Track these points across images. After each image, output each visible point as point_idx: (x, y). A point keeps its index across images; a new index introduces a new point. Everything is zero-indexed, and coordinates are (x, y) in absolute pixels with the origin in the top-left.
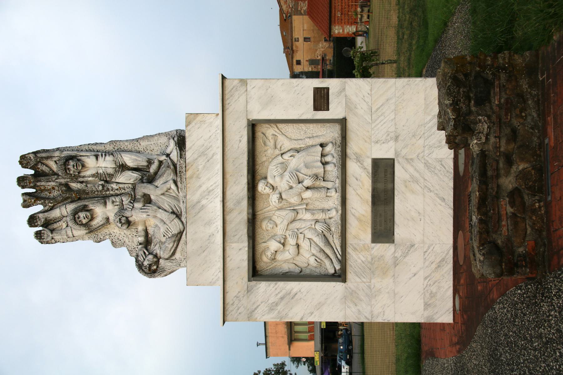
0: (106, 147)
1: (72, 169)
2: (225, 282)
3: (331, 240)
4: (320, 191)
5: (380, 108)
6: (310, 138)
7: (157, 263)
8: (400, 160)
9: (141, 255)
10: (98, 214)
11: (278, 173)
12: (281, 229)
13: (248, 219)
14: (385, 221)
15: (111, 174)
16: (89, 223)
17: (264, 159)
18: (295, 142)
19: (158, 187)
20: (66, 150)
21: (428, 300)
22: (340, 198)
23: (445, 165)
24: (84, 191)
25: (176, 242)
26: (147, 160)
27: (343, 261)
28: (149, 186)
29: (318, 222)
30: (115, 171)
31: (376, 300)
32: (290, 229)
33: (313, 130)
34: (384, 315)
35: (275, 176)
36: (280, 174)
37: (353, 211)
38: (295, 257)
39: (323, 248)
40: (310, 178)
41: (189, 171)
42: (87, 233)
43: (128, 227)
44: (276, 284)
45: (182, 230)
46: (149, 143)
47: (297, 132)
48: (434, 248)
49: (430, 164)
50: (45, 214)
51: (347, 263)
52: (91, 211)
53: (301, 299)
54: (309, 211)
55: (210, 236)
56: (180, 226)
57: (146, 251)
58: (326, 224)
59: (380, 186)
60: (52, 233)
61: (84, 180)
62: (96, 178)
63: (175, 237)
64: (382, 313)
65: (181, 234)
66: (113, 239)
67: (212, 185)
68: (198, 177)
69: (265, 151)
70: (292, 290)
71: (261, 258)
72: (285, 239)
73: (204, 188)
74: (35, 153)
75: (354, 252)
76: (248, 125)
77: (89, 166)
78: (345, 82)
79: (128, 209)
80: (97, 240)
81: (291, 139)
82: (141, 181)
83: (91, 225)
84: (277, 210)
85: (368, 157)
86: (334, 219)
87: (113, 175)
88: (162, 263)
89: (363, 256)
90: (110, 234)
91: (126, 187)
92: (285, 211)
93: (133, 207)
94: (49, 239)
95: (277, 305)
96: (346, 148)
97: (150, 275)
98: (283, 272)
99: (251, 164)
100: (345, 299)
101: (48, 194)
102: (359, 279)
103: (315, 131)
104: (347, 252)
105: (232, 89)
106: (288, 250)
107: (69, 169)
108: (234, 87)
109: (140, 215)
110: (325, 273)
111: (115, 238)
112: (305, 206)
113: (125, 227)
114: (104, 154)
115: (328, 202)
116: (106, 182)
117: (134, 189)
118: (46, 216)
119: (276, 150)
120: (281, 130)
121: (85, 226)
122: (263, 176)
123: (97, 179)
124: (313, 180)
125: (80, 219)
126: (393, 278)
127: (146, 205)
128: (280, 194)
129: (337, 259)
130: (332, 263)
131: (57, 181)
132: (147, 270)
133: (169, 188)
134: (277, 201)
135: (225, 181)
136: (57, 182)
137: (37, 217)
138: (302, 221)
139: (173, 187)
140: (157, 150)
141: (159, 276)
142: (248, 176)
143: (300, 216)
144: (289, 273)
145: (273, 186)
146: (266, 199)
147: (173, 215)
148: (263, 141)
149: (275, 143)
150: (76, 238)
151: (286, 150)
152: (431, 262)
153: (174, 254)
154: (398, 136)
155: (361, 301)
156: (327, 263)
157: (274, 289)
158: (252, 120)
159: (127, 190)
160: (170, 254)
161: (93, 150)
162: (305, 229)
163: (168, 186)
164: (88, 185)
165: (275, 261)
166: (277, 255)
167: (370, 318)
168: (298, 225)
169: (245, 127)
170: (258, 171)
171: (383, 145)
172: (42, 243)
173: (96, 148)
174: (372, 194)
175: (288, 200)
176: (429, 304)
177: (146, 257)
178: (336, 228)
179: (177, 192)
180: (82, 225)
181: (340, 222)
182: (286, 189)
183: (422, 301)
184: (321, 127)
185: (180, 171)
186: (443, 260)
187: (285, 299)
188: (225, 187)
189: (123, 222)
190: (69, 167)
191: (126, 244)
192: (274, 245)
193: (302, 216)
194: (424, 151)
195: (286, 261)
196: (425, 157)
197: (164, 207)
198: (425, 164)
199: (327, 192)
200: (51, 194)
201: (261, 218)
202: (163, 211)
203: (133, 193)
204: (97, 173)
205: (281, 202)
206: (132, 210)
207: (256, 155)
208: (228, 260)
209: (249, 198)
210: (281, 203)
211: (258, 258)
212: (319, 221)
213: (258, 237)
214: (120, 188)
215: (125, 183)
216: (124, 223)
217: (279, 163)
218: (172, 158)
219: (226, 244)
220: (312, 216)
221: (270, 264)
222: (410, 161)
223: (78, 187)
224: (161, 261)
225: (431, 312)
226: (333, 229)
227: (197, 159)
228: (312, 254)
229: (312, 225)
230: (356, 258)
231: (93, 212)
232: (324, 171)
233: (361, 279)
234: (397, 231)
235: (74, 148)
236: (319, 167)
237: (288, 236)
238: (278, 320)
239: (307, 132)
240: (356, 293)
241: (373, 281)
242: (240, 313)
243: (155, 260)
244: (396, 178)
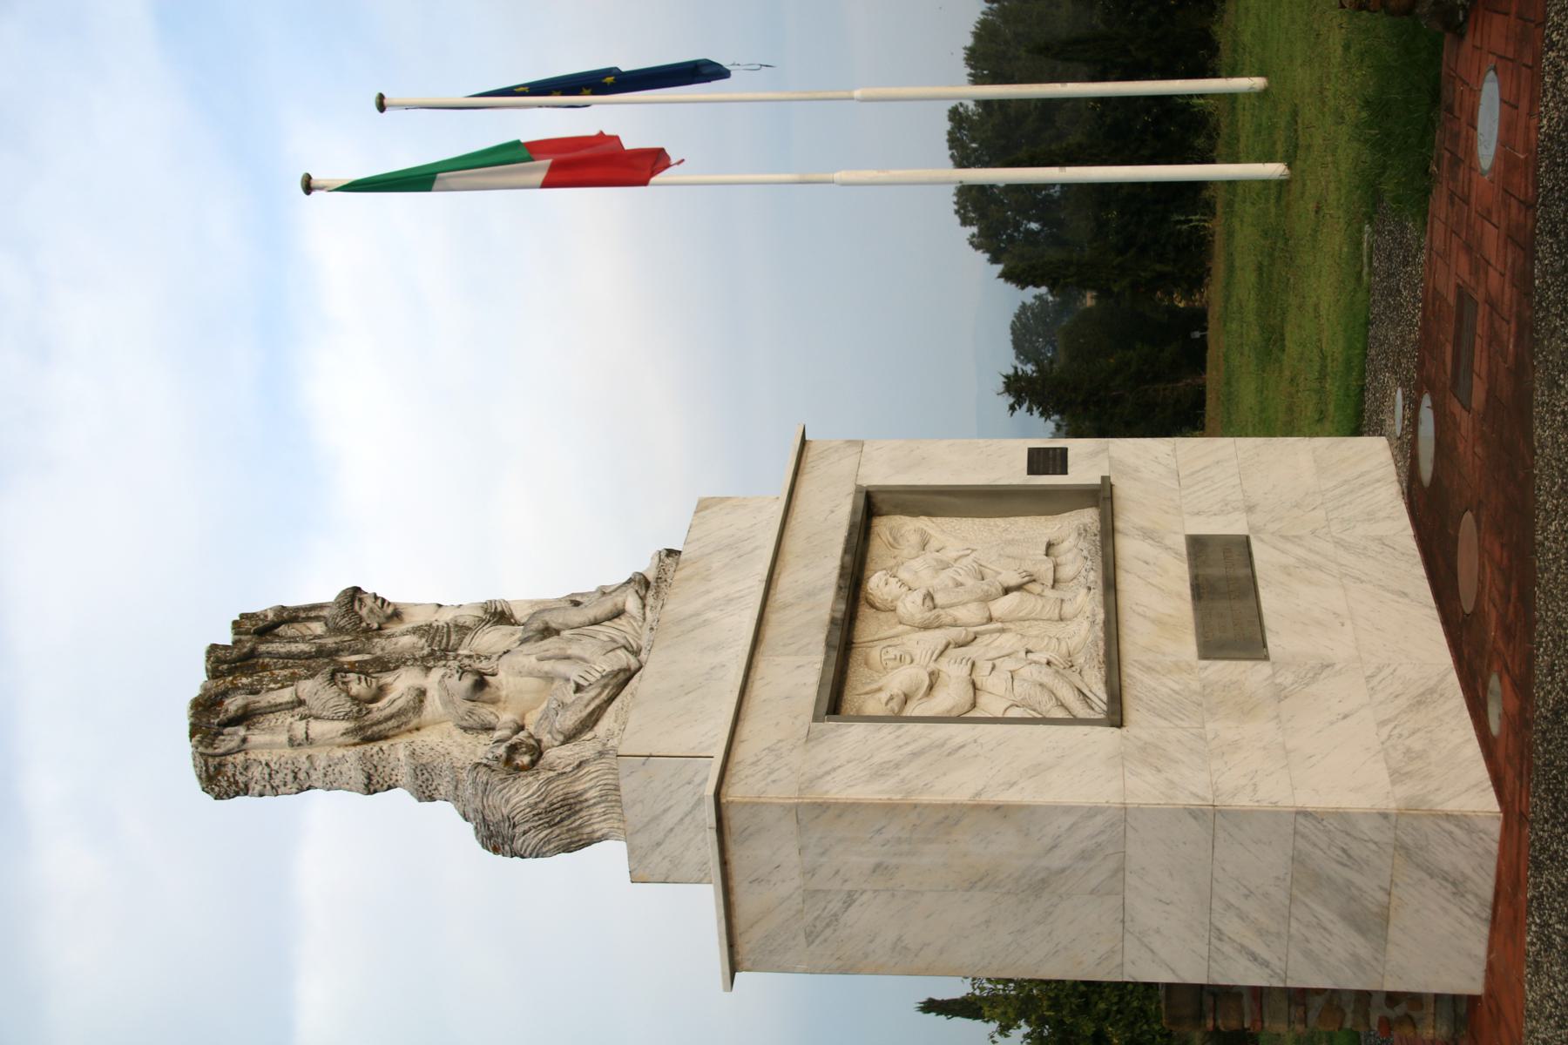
2: (740, 723)
5: (1199, 471)
13: (833, 621)
21: (1403, 764)
25: (610, 687)
31: (1226, 763)
34: (1255, 790)
44: (900, 728)
48: (1395, 670)
55: (712, 669)
59: (1215, 571)
65: (628, 674)
67: (740, 591)
75: (1146, 676)
87: (469, 629)
95: (897, 766)
100: (1123, 758)
107: (361, 600)
135: (779, 563)
142: (843, 558)
153: (590, 721)
155: (1177, 762)
157: (893, 736)
167: (1210, 797)
174: (1192, 585)
176: (1407, 773)
181: (1101, 635)
186: (1432, 691)
209: (840, 588)
233: (1170, 722)
238: (897, 797)
241: (1210, 726)
242: (774, 781)
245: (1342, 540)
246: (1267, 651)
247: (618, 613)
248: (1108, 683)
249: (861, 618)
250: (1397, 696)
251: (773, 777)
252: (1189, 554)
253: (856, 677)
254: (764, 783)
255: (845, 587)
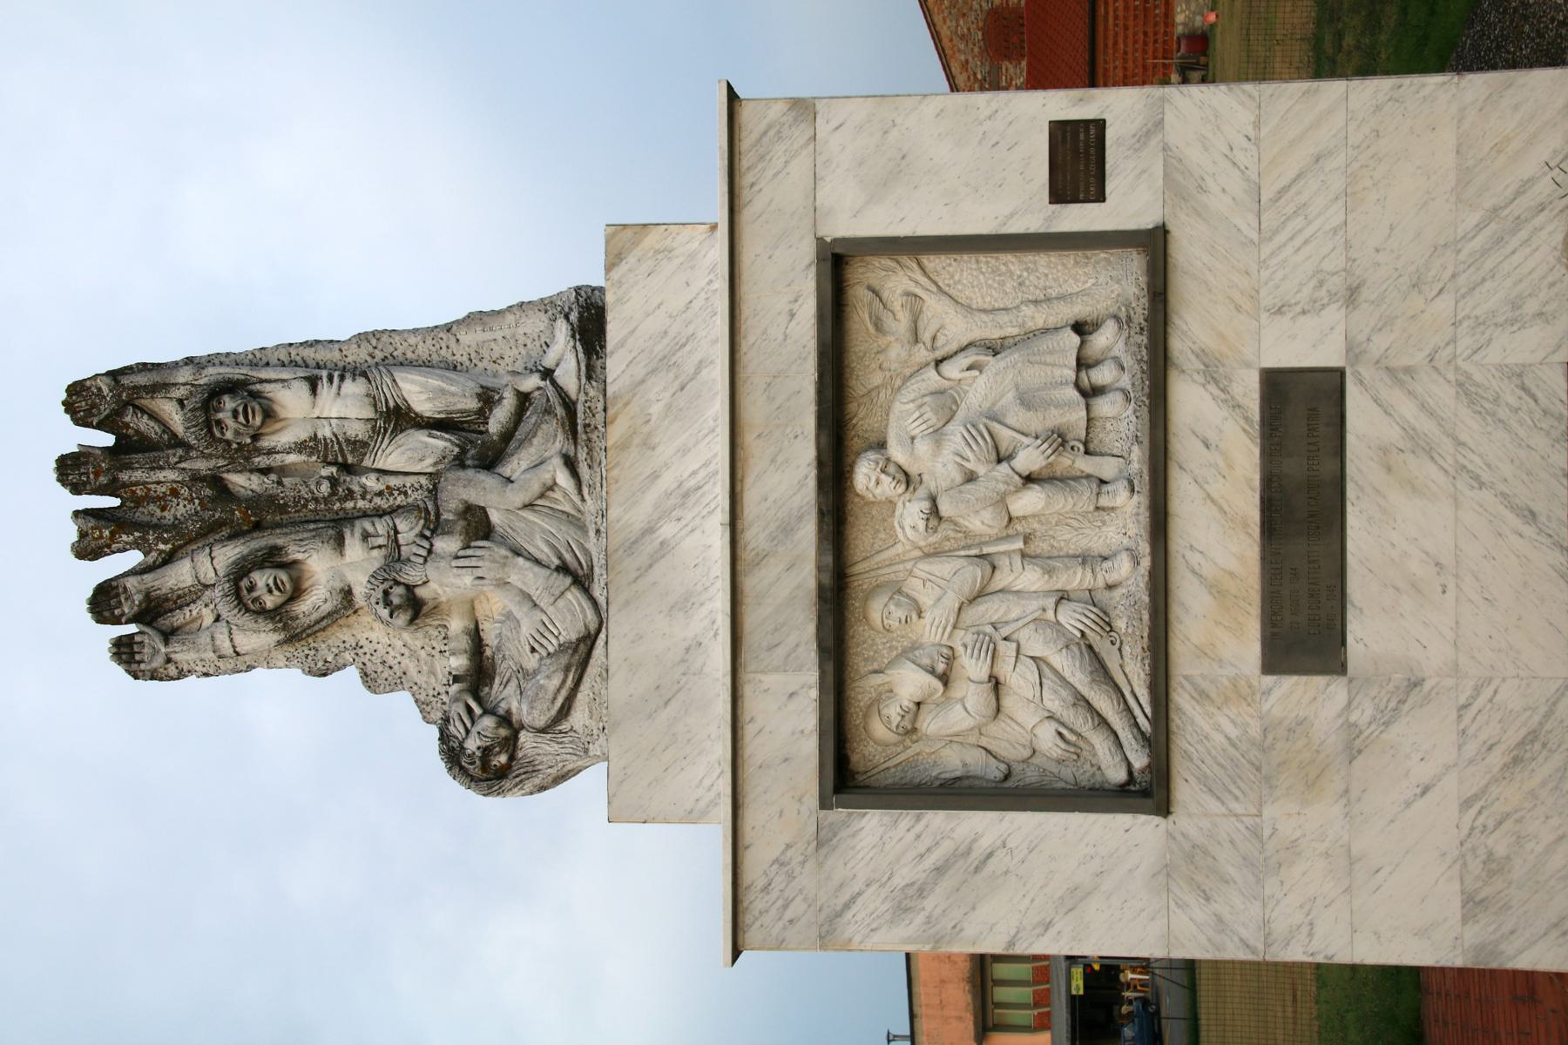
0: (344, 353)
1: (230, 422)
2: (740, 812)
3: (1113, 664)
4: (1073, 490)
6: (1036, 302)
7: (511, 743)
8: (1366, 372)
9: (456, 718)
10: (316, 576)
11: (924, 426)
12: (936, 623)
13: (821, 588)
14: (1312, 596)
15: (361, 442)
16: (288, 607)
17: (877, 379)
18: (984, 317)
19: (512, 482)
20: (217, 362)
22: (1147, 514)
23: (1534, 390)
24: (272, 499)
25: (573, 670)
26: (479, 390)
27: (1159, 740)
28: (485, 479)
29: (1068, 600)
30: (374, 432)
31: (1282, 883)
32: (969, 622)
33: (1046, 275)
34: (1310, 935)
35: (913, 439)
36: (931, 430)
37: (1195, 559)
38: (986, 724)
39: (1086, 695)
40: (1039, 442)
41: (618, 421)
42: (279, 643)
43: (412, 621)
44: (918, 819)
45: (593, 627)
46: (488, 336)
47: (990, 282)
48: (1496, 692)
49: (1478, 385)
50: (145, 576)
51: (1173, 747)
52: (295, 566)
53: (1006, 873)
54: (1034, 561)
55: (688, 650)
56: (585, 616)
57: (473, 705)
58: (1095, 605)
59: (1294, 467)
60: (166, 642)
61: (273, 464)
62: (311, 455)
63: (570, 651)
64: (1305, 930)
65: (589, 643)
66: (366, 661)
67: (694, 473)
68: (648, 445)
69: (878, 352)
70: (975, 840)
71: (864, 728)
72: (951, 659)
73: (667, 481)
74: (114, 375)
75: (1197, 708)
76: (820, 258)
77: (289, 416)
78: (1163, 99)
79: (413, 558)
80: (313, 666)
81: (969, 309)
82: (457, 462)
83: (293, 614)
84: (920, 558)
85: (1248, 365)
86: (1124, 591)
87: (365, 444)
88: (528, 745)
89: (1233, 721)
90: (358, 646)
91: (408, 485)
92: (949, 559)
93: (430, 552)
94: (158, 662)
95: (921, 893)
96: (1165, 332)
97: (485, 784)
98: (943, 776)
99: (829, 393)
100: (1168, 875)
101: (158, 511)
102: (1219, 804)
103: (1055, 280)
104: (1172, 706)
105: (765, 133)
106: (962, 701)
107: (219, 422)
108: (770, 127)
109: (453, 580)
110: (1092, 781)
111: (373, 658)
112: (1020, 545)
113: (402, 619)
114: (336, 374)
115: (1104, 529)
116: (346, 468)
117: (434, 492)
118: (149, 585)
119: (916, 348)
120: (937, 279)
121: (272, 619)
122: (873, 438)
123: (314, 458)
124: (1050, 451)
125: (255, 594)
126: (1344, 801)
127: (473, 544)
128: (933, 500)
129: (1135, 731)
130: (1120, 745)
131: (183, 465)
132: (475, 770)
133: (550, 483)
134: (921, 525)
135: (740, 453)
136: (184, 469)
137: (121, 590)
138: (1011, 597)
139: (563, 479)
140: (513, 357)
141: (516, 790)
143: (1001, 580)
144: (966, 783)
145: (906, 474)
146: (884, 520)
147: (561, 575)
148: (871, 318)
149: (915, 322)
150: (247, 658)
151: (954, 347)
152: (1487, 745)
153: (565, 711)
154: (1358, 287)
155: (1227, 882)
156: (1101, 745)
157: (911, 835)
158: (835, 240)
159: (414, 497)
160: (554, 712)
161: (304, 361)
162: (1020, 623)
163: (547, 477)
164: (284, 480)
165: (915, 737)
166: (921, 718)
167: (1261, 947)
168: (997, 610)
169: (810, 265)
170: (854, 421)
171: (1302, 319)
172: (136, 678)
173: (312, 355)
174: (1262, 498)
175: (961, 521)
176: (1482, 901)
177: (473, 723)
178: (1131, 624)
179: (576, 499)
180: (262, 612)
181: (1146, 599)
182: (952, 481)
183: (1456, 886)
184: (1076, 263)
185: (586, 426)
187: (951, 872)
188: (739, 476)
189: (396, 601)
190: (220, 415)
191: (408, 681)
192: (910, 682)
193: (1011, 579)
194: (1453, 341)
195: (955, 739)
196: (1459, 362)
197: (532, 550)
198: (1460, 385)
199: (1098, 494)
200: (166, 513)
201: (865, 587)
202: (528, 564)
203: (430, 507)
204: (315, 438)
205: (935, 530)
206: (426, 561)
207: (847, 366)
208: (749, 731)
209: (821, 514)
210: (935, 532)
211: (856, 726)
212: (1072, 596)
213: (857, 654)
214: (388, 487)
215: (407, 474)
216: (399, 607)
217: (927, 392)
218: (560, 381)
219: (744, 676)
220: (1046, 576)
221: (899, 750)
222: (1401, 376)
223: (254, 487)
224: (524, 737)
225: (1491, 929)
226: (1121, 624)
227: (643, 381)
228: (1047, 714)
229: (1044, 610)
230: (1207, 728)
231: (302, 571)
232: (1088, 420)
233: (1223, 803)
234: (1356, 629)
235: (243, 356)
236: (1069, 404)
237: (960, 649)
239: (1027, 283)
240: (1206, 853)
241: (1268, 811)
242: (791, 921)
243: (503, 732)
244: (1351, 439)
245: (1469, 376)
246: (1345, 653)
247: (552, 486)
248: (1153, 688)
249: (851, 519)
250: (1490, 749)
251: (788, 915)
252: (1264, 422)
253: (858, 645)
254: (780, 924)
255: (828, 511)
